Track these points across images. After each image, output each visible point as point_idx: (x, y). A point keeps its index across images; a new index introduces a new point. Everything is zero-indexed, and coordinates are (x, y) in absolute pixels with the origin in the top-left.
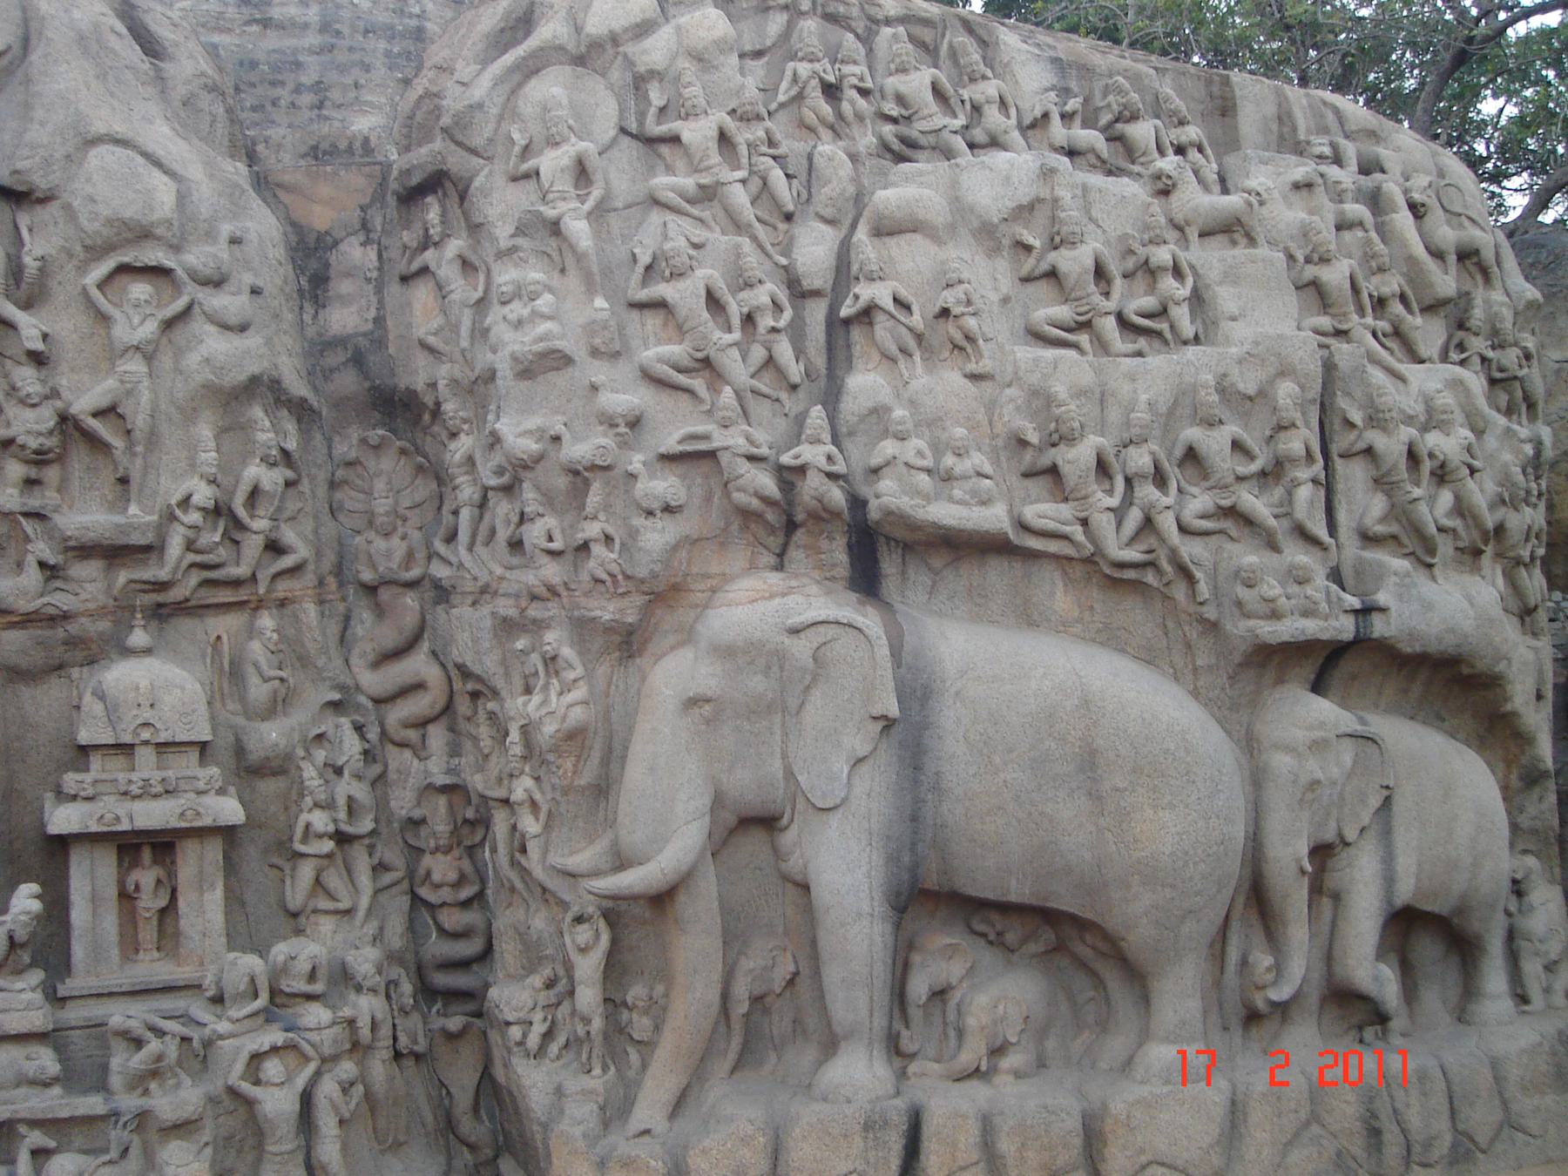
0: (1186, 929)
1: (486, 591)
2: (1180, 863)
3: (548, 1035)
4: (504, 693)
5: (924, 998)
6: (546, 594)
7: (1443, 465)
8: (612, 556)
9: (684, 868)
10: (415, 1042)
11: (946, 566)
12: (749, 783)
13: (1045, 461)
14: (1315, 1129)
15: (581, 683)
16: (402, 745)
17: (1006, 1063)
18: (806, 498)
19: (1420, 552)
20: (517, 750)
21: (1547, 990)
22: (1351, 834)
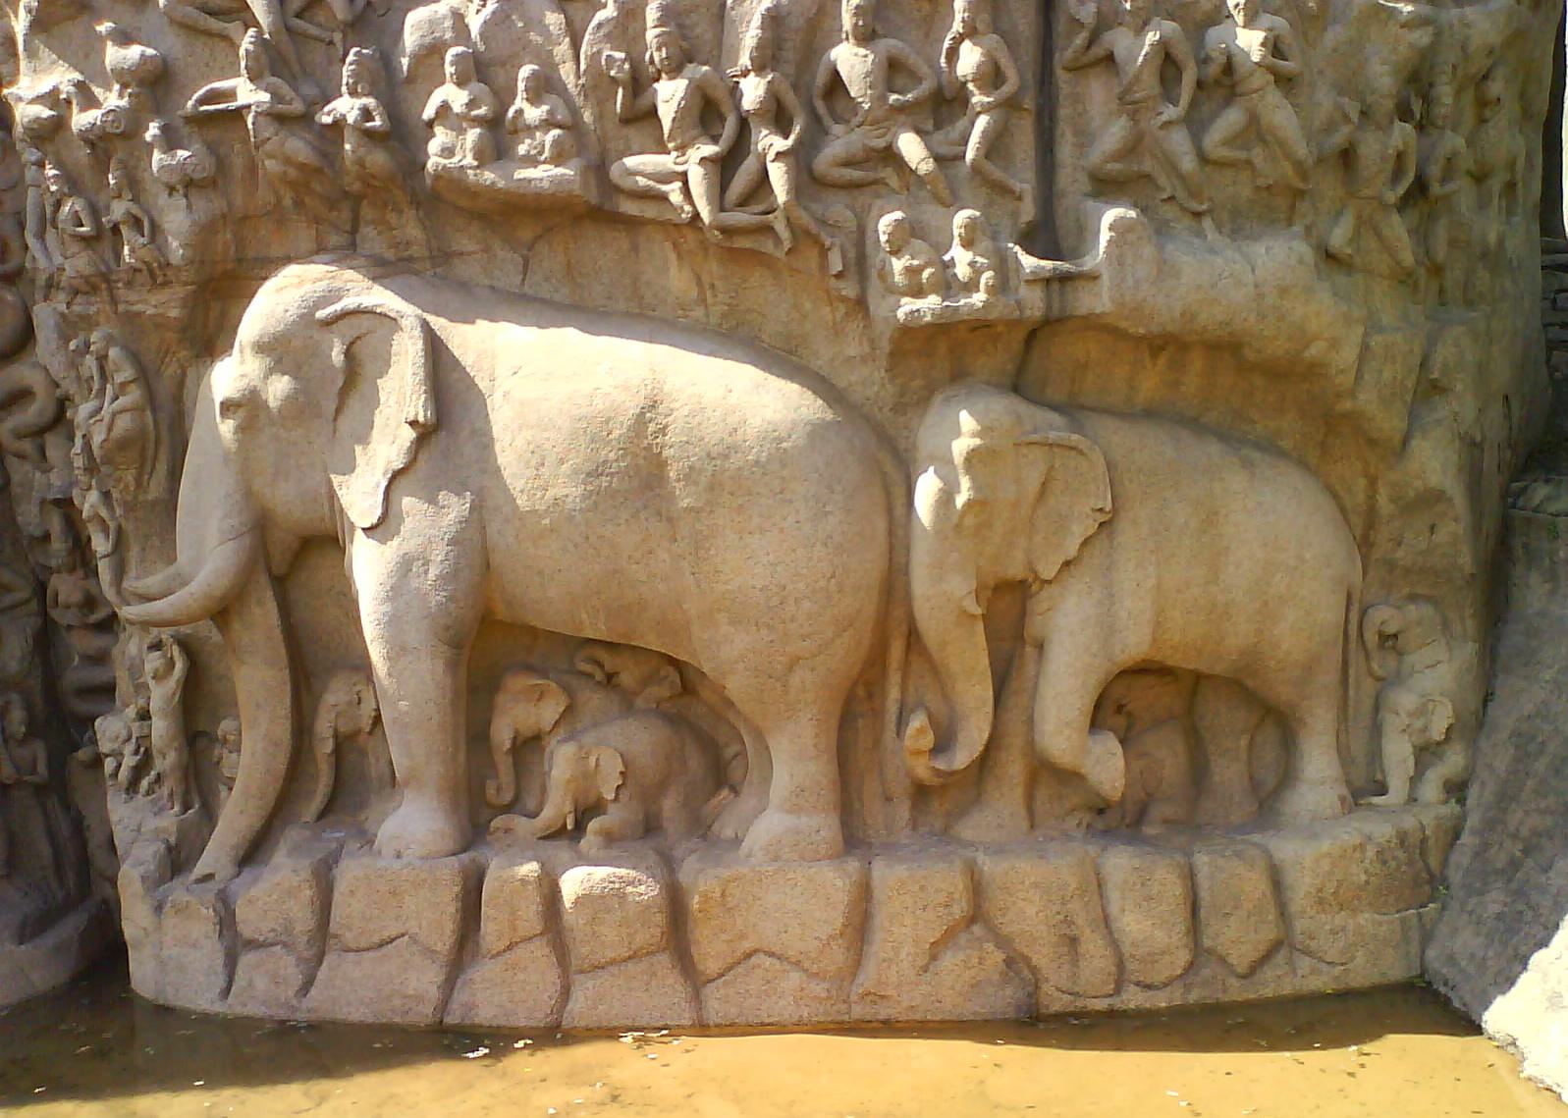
0: (795, 680)
1: (51, 285)
2: (775, 601)
3: (139, 771)
4: (77, 399)
5: (508, 745)
6: (85, 288)
7: (1229, 68)
8: (142, 240)
9: (218, 593)
10: (34, 771)
11: (539, 238)
12: (286, 499)
13: (643, 102)
14: (977, 929)
15: (133, 387)
16: (21, 456)
17: (593, 825)
18: (348, 163)
19: (1181, 194)
20: (79, 462)
21: (1415, 780)
22: (1048, 571)
